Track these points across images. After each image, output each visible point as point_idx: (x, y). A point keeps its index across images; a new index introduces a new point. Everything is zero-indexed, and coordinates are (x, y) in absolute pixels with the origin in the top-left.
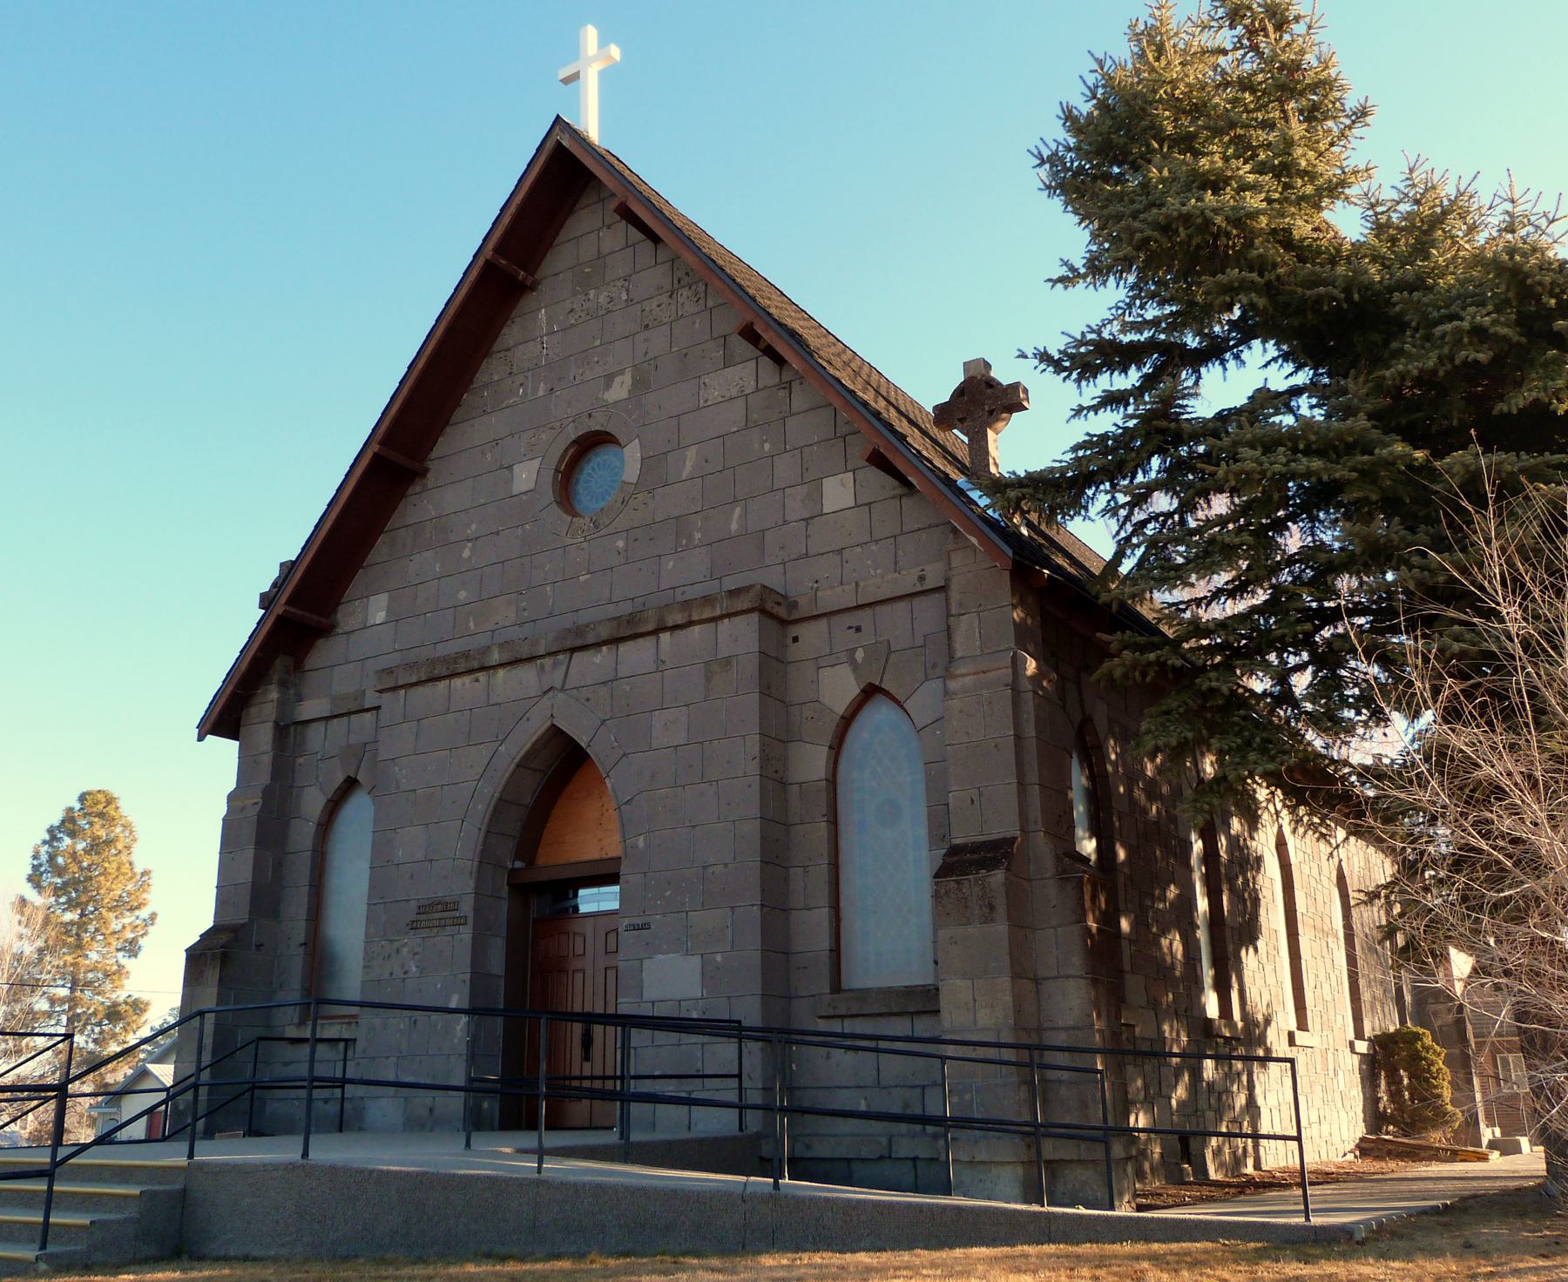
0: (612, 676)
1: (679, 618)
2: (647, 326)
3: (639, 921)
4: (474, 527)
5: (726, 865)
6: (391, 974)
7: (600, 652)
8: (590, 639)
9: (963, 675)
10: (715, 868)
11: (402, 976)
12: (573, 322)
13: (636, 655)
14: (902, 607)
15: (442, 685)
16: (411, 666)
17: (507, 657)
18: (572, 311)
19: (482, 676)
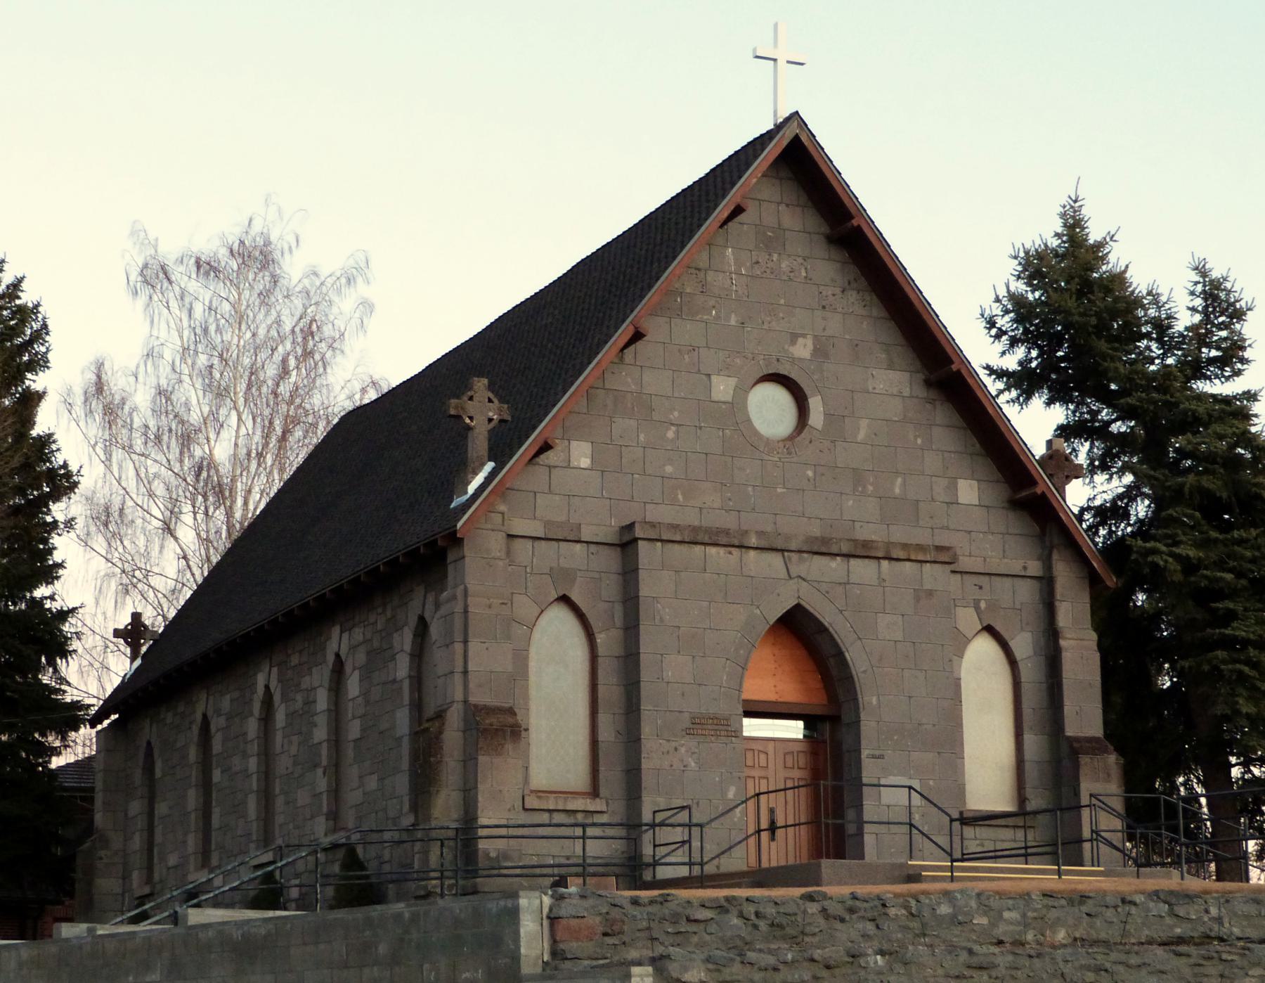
0: (845, 580)
1: (902, 555)
2: (824, 307)
3: (877, 753)
4: (676, 414)
5: (934, 725)
6: (672, 766)
7: (836, 559)
8: (834, 550)
9: (1070, 639)
10: (925, 726)
11: (682, 768)
12: (759, 273)
13: (862, 570)
14: (1008, 581)
15: (698, 549)
16: (675, 527)
17: (763, 544)
18: (757, 262)
19: (735, 551)
